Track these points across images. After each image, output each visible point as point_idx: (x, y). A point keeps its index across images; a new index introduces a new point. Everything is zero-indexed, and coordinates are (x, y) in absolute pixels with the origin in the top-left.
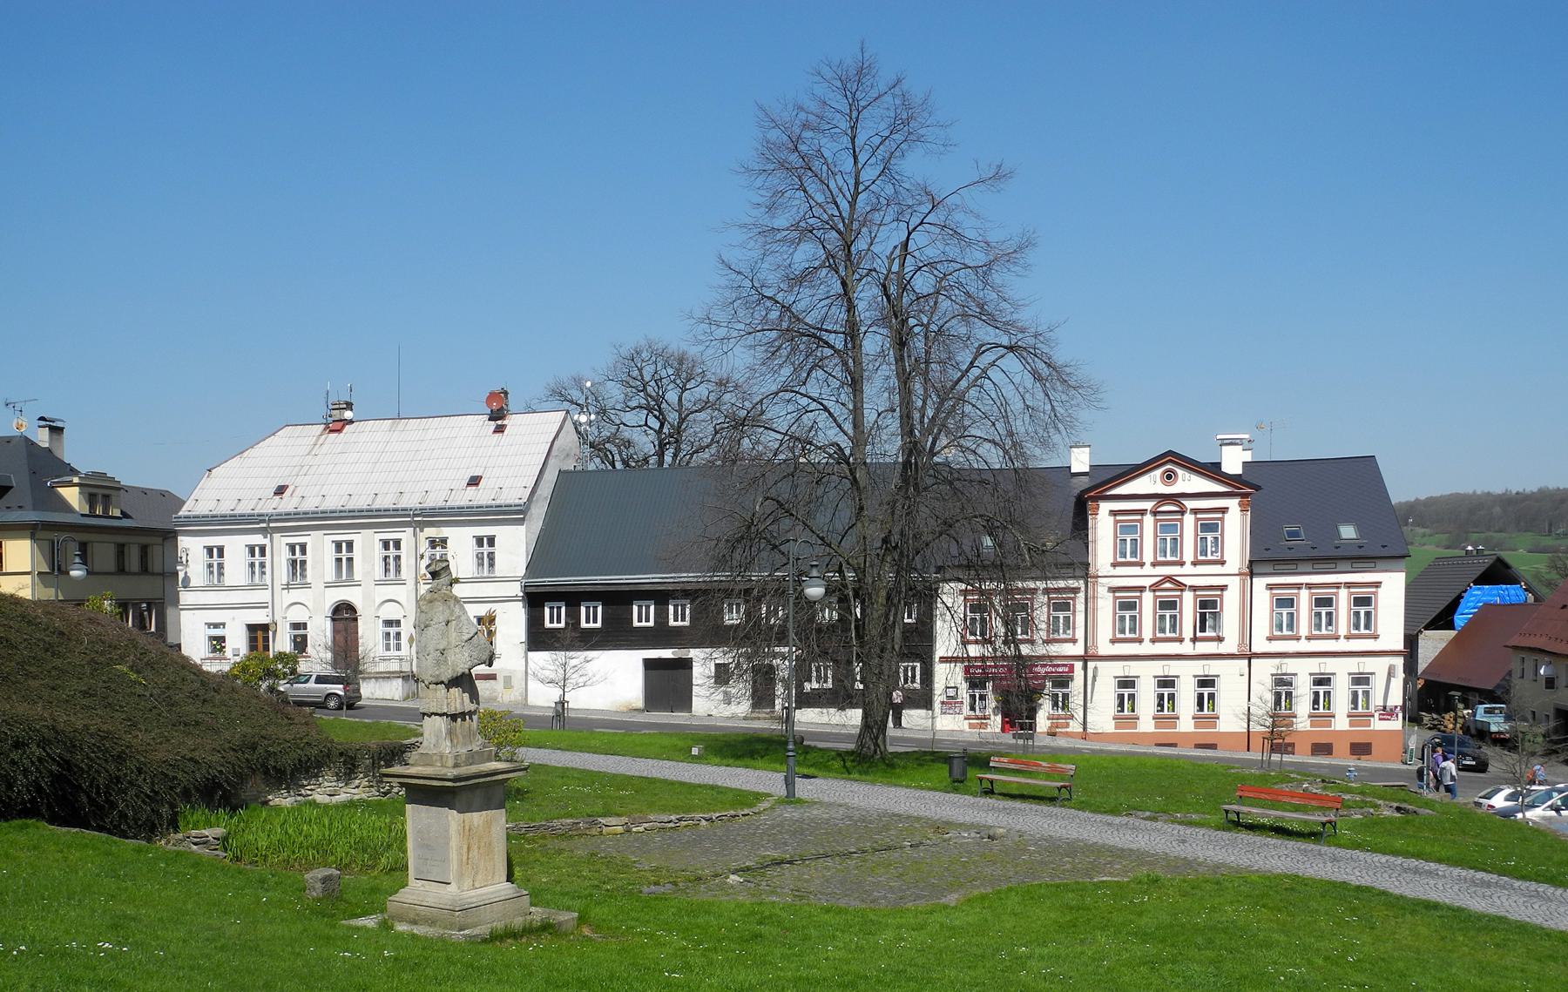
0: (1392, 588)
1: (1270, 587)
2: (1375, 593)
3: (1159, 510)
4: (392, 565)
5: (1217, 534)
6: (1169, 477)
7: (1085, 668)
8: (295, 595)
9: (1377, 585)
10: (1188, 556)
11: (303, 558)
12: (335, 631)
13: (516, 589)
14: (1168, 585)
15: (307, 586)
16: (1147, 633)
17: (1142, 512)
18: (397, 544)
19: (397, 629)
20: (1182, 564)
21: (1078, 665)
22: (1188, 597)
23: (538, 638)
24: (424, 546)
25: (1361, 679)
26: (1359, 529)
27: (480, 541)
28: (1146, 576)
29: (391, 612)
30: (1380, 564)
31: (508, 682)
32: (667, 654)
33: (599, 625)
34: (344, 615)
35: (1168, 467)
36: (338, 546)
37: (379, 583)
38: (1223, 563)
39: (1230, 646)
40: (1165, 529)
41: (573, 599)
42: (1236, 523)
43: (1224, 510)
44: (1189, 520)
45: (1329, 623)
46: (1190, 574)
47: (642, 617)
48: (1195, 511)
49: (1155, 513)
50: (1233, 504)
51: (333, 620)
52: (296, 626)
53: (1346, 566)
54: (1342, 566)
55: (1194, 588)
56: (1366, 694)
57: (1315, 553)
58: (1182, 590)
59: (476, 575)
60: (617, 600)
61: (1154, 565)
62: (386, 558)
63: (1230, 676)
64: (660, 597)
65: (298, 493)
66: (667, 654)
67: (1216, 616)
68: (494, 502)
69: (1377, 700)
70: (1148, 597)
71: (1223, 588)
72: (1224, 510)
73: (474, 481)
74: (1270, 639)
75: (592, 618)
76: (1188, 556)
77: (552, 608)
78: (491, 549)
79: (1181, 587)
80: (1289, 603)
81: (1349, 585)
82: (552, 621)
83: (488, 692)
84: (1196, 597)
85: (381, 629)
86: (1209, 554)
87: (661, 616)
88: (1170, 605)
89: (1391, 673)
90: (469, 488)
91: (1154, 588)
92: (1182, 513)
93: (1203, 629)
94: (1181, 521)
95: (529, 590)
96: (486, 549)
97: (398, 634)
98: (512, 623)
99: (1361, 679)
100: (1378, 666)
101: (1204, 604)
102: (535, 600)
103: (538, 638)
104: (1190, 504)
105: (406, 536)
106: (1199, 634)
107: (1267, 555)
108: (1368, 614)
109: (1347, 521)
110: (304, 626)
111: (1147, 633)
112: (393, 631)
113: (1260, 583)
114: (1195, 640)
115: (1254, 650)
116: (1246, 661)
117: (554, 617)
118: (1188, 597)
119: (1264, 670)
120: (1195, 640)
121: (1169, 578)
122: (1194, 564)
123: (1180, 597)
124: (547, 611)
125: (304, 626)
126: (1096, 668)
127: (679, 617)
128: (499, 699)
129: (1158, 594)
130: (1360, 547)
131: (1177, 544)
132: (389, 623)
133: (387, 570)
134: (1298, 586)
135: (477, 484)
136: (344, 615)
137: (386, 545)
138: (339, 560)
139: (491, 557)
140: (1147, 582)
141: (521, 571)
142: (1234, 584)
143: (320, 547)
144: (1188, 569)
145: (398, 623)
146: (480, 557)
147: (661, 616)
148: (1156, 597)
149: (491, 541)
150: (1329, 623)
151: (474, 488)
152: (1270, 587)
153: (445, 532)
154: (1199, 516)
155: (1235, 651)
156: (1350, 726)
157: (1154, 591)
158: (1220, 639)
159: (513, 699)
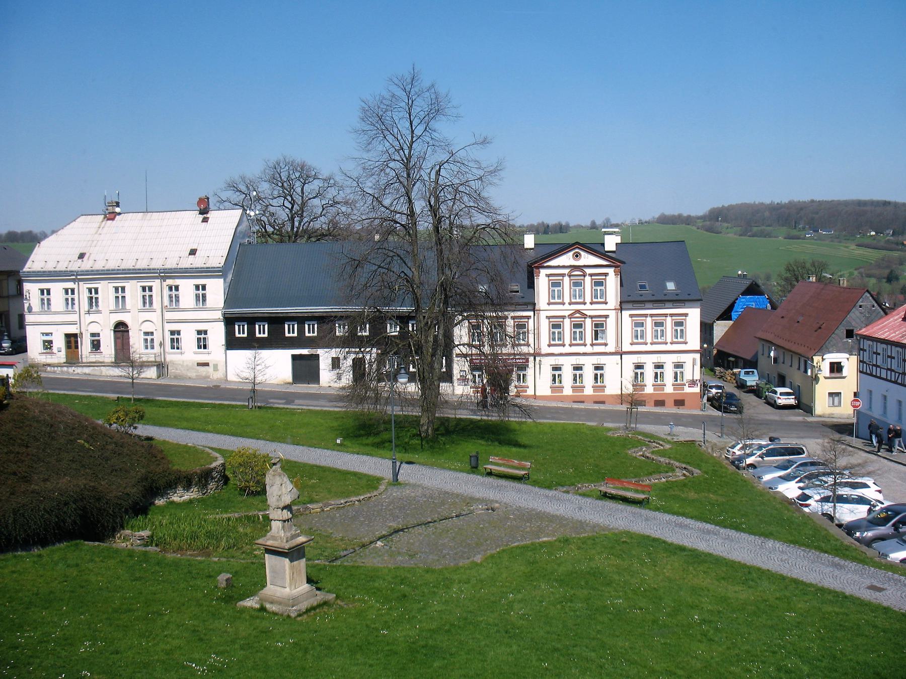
0: (693, 316)
1: (631, 316)
2: (685, 320)
3: (572, 274)
4: (147, 301)
5: (603, 288)
6: (577, 256)
7: (535, 359)
8: (93, 317)
9: (686, 315)
10: (588, 300)
11: (96, 296)
12: (116, 338)
13: (219, 315)
14: (578, 315)
15: (99, 312)
16: (567, 341)
17: (563, 275)
18: (150, 289)
19: (152, 337)
20: (585, 304)
21: (531, 359)
22: (588, 321)
23: (232, 343)
24: (166, 292)
25: (679, 366)
26: (677, 285)
27: (197, 287)
28: (566, 310)
29: (148, 327)
30: (687, 304)
31: (216, 368)
32: (305, 352)
33: (266, 335)
34: (121, 329)
35: (577, 250)
36: (117, 289)
37: (140, 311)
38: (606, 303)
39: (611, 348)
40: (577, 284)
41: (251, 321)
42: (612, 282)
43: (606, 274)
44: (588, 279)
45: (662, 336)
46: (589, 309)
47: (290, 331)
48: (591, 275)
49: (570, 276)
50: (611, 271)
51: (115, 332)
52: (93, 335)
53: (670, 305)
54: (667, 305)
55: (591, 317)
56: (682, 373)
57: (654, 298)
58: (585, 318)
59: (195, 307)
60: (276, 322)
61: (570, 304)
62: (144, 297)
63: (611, 363)
64: (301, 320)
65: (92, 258)
66: (305, 352)
67: (604, 332)
68: (205, 266)
69: (688, 376)
70: (567, 322)
71: (607, 317)
72: (606, 274)
73: (193, 252)
74: (631, 344)
75: (262, 332)
76: (588, 299)
77: (239, 326)
78: (204, 292)
79: (585, 316)
80: (642, 325)
81: (672, 315)
82: (239, 333)
83: (205, 373)
84: (592, 321)
85: (143, 337)
86: (599, 298)
87: (301, 331)
88: (578, 326)
89: (694, 360)
90: (190, 256)
91: (570, 316)
92: (584, 276)
93: (596, 339)
94: (584, 280)
95: (226, 316)
96: (201, 292)
97: (152, 340)
98: (217, 334)
99: (679, 366)
100: (687, 359)
101: (596, 326)
102: (230, 321)
103: (232, 343)
104: (588, 271)
105: (156, 284)
106: (595, 342)
107: (630, 299)
108: (682, 331)
109: (670, 280)
110: (98, 335)
111: (567, 341)
112: (149, 338)
113: (626, 314)
114: (592, 345)
115: (623, 350)
116: (620, 356)
117: (241, 332)
118: (588, 321)
119: (629, 361)
120: (592, 345)
121: (578, 311)
122: (591, 303)
123: (584, 321)
124: (237, 327)
125: (98, 335)
126: (540, 361)
127: (312, 330)
128: (211, 377)
129: (572, 320)
130: (677, 295)
131: (582, 294)
132: (146, 334)
133: (144, 303)
134: (646, 316)
135: (195, 254)
136: (121, 329)
137: (144, 289)
138: (117, 297)
139: (204, 296)
140: (567, 313)
141: (222, 305)
142: (612, 315)
143: (106, 290)
144: (588, 306)
145: (152, 333)
146: (197, 296)
147: (301, 331)
148: (571, 321)
149: (204, 287)
150: (662, 336)
151: (193, 256)
152: (631, 316)
153: (178, 282)
154: (593, 277)
155: (613, 350)
156: (674, 390)
157: (571, 318)
158: (606, 345)
159: (219, 377)
